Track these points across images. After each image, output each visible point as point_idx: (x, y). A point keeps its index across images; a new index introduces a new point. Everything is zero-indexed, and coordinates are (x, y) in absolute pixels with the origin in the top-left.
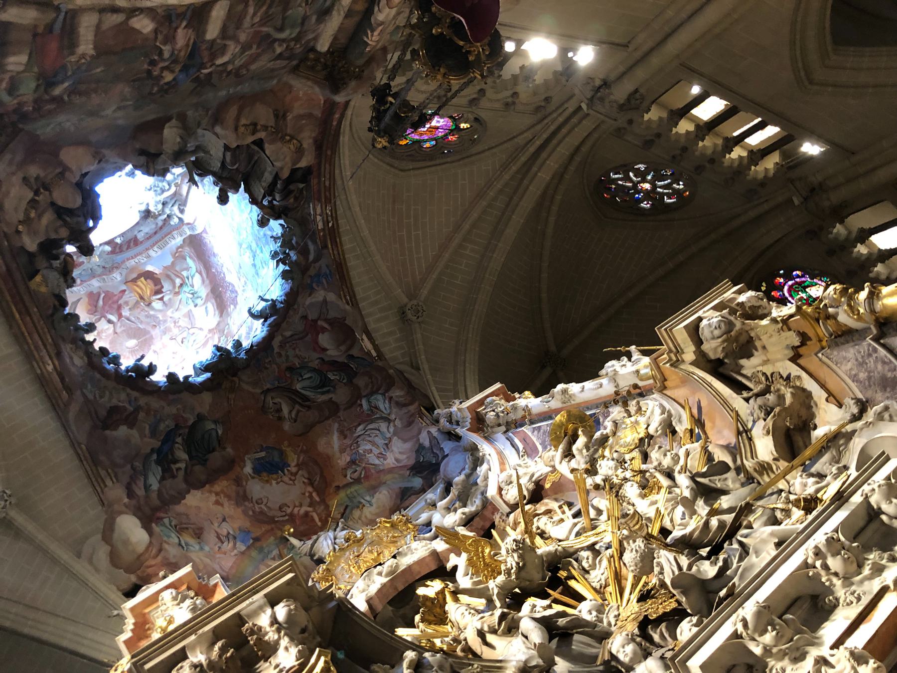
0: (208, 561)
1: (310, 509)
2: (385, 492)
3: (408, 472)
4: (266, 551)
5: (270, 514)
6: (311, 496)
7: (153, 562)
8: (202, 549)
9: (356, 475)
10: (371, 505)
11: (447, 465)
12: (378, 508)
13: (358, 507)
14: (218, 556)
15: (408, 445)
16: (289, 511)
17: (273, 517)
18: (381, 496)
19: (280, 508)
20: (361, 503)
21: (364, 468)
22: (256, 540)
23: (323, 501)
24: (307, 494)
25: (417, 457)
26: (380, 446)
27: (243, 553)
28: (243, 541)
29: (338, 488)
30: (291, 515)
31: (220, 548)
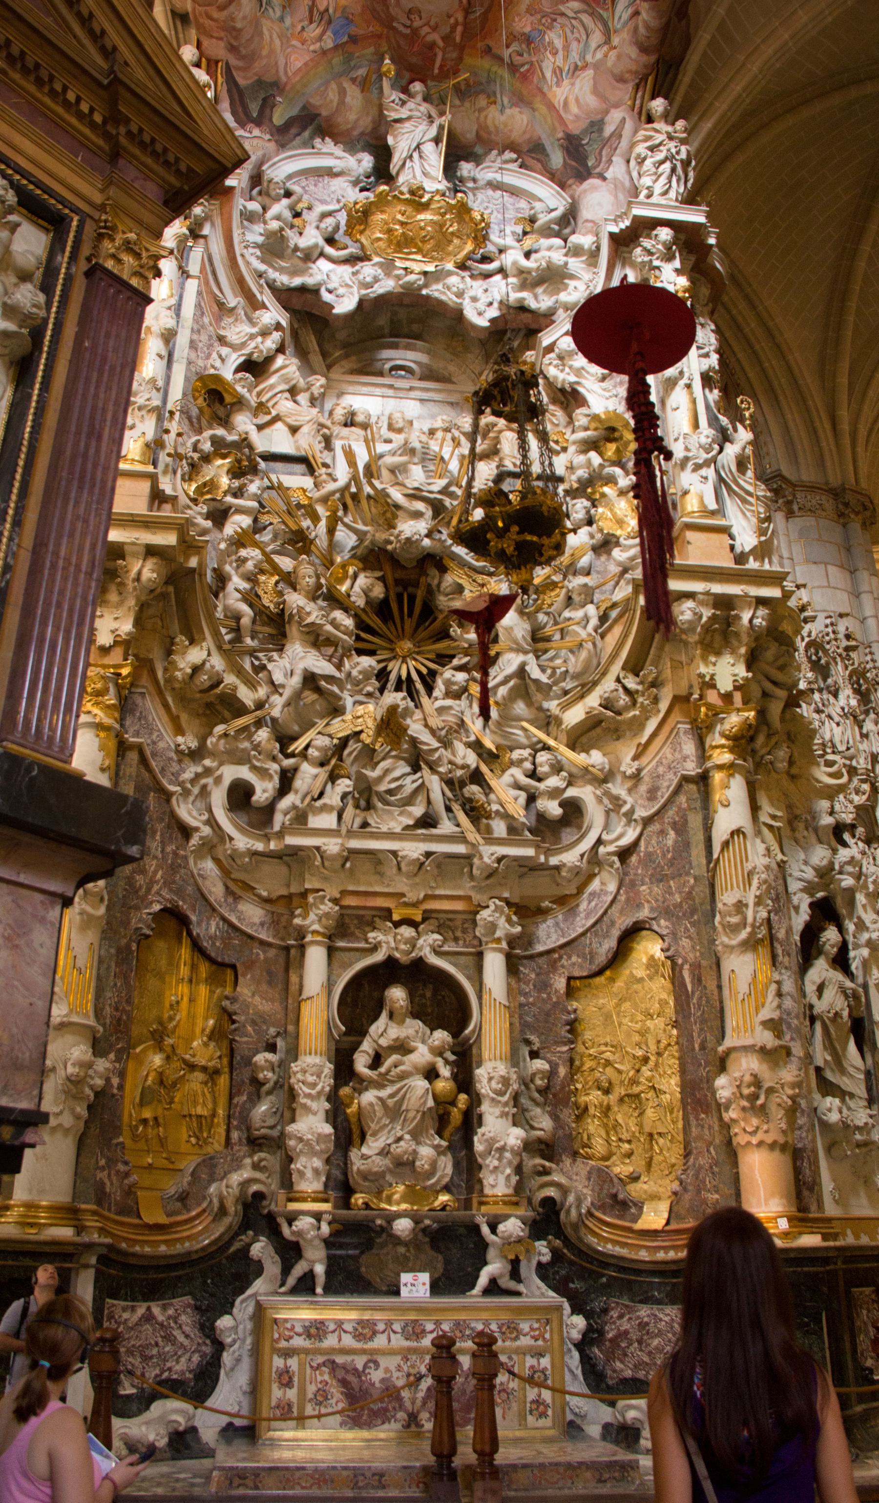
0: (277, 42)
1: (441, 43)
2: (525, 117)
3: (560, 135)
4: (352, 63)
5: (393, 11)
6: (453, 28)
7: (216, 15)
8: (282, 19)
9: (517, 59)
10: (502, 112)
11: (594, 188)
12: (506, 125)
13: (489, 97)
14: (294, 42)
15: (592, 102)
16: (417, 23)
17: (393, 19)
18: (518, 117)
19: (410, 12)
20: (495, 93)
21: (532, 64)
22: (354, 40)
23: (461, 48)
24: (452, 21)
25: (585, 131)
26: (571, 60)
27: (324, 53)
28: (335, 34)
29: (488, 51)
30: (415, 32)
31: (303, 28)
